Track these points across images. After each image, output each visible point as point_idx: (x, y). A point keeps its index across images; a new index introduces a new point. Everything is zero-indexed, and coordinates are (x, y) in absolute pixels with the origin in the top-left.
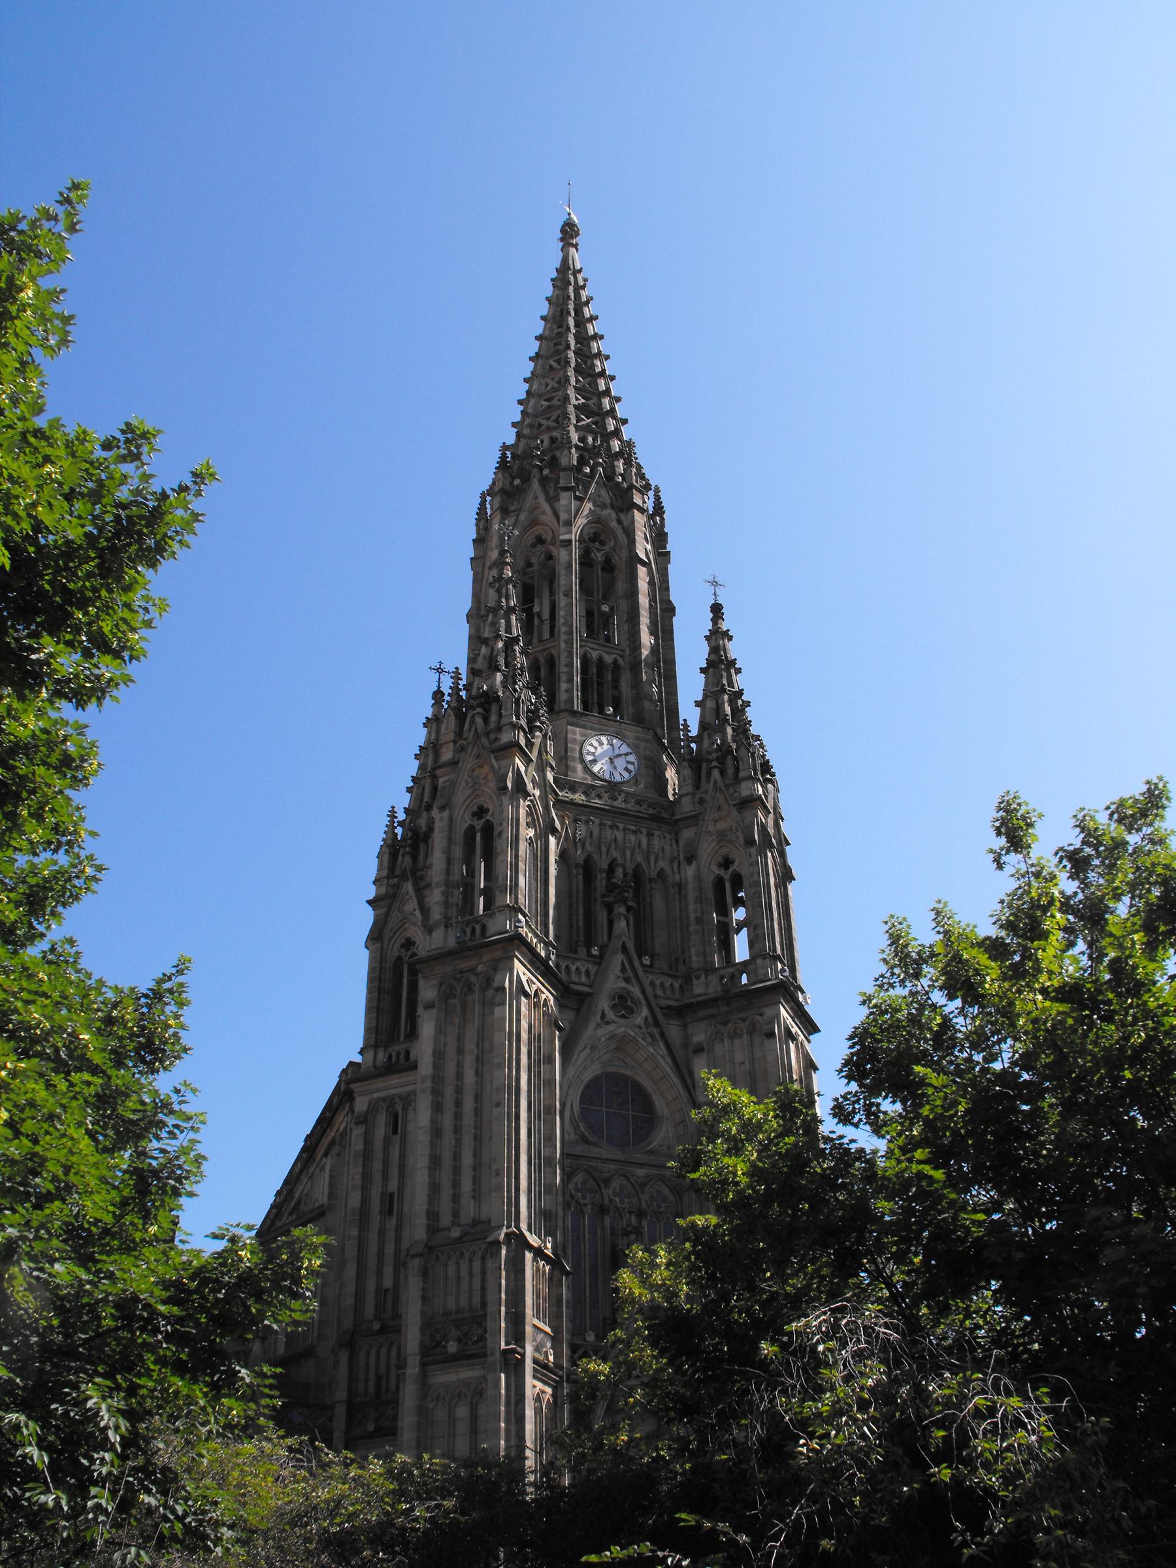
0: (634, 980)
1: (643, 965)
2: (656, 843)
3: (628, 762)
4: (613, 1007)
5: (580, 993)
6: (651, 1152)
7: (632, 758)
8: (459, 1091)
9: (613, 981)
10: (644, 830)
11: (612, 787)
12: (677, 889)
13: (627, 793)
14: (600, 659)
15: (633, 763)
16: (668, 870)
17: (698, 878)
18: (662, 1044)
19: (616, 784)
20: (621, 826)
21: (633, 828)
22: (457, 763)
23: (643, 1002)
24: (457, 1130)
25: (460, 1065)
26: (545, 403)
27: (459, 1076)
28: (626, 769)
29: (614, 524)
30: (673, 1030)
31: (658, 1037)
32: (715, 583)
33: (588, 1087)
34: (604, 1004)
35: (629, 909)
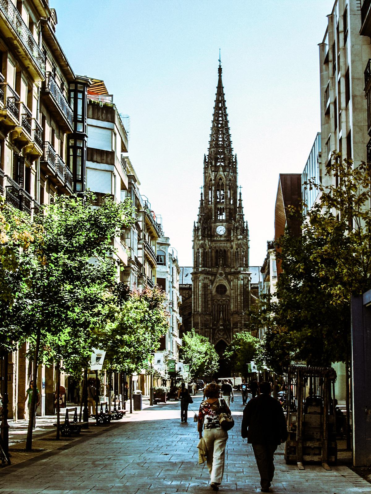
4: (220, 275)
7: (225, 229)
9: (220, 271)
11: (221, 236)
30: (229, 277)
34: (218, 275)
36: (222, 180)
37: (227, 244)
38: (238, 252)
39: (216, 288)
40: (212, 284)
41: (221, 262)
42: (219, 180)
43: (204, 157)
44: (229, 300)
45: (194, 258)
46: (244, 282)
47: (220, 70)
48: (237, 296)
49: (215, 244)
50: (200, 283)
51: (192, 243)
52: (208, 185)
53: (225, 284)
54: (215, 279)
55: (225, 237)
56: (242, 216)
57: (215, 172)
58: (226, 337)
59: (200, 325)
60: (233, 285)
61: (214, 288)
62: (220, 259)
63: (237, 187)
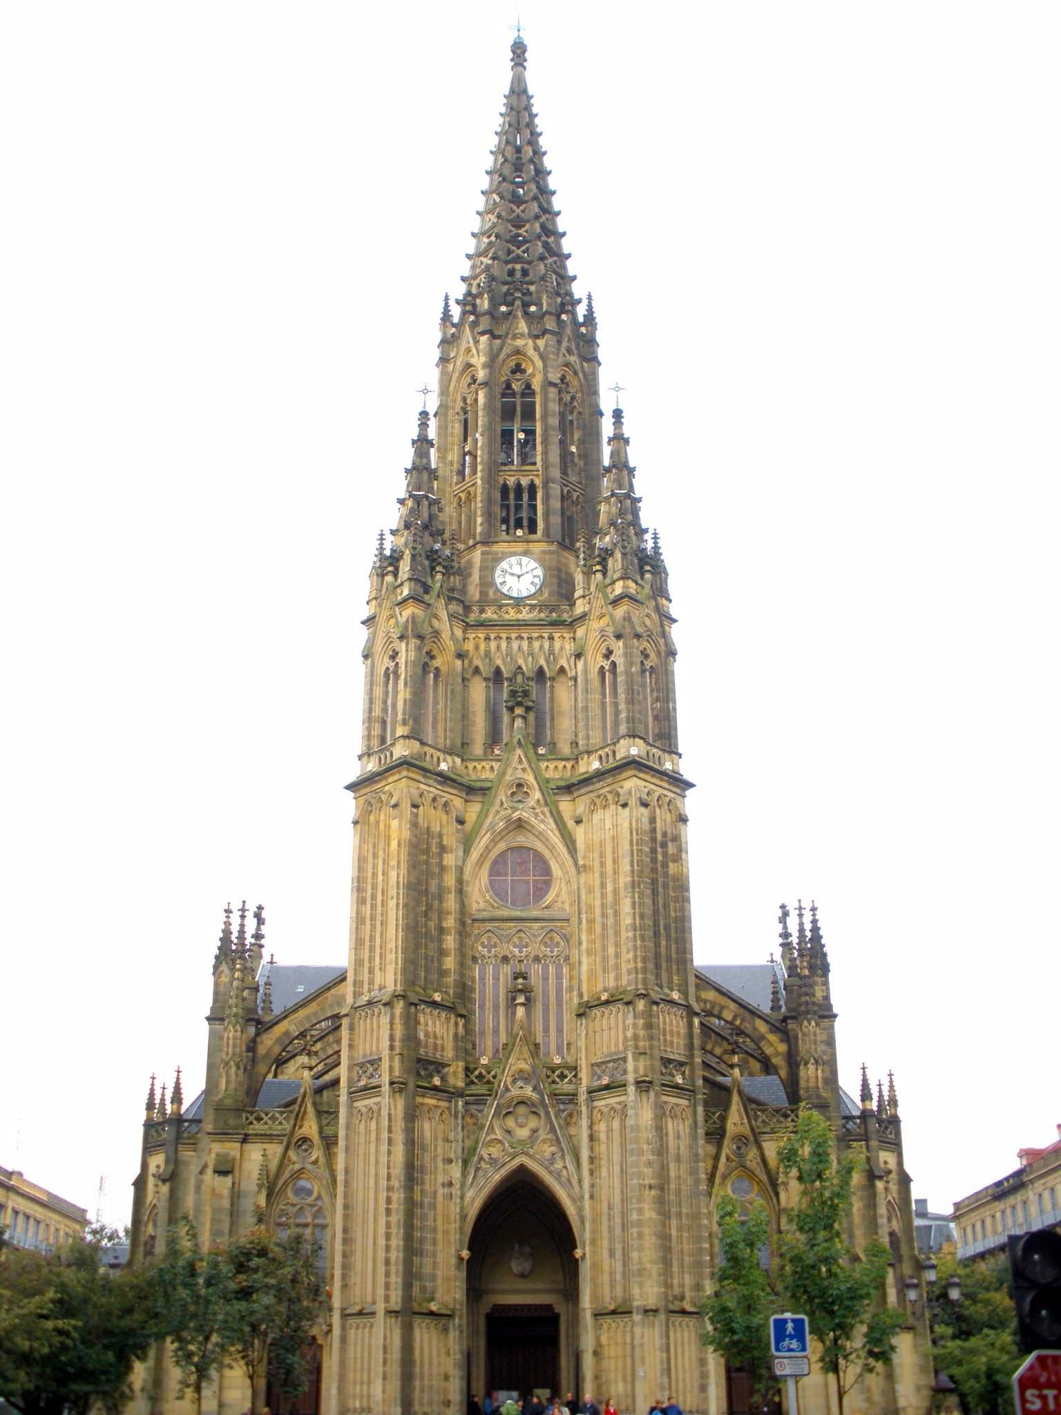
0: (529, 770)
1: (536, 753)
2: (557, 644)
3: (534, 576)
5: (482, 789)
6: (547, 907)
8: (374, 887)
10: (546, 635)
11: (518, 602)
12: (573, 683)
13: (532, 606)
14: (519, 487)
15: (539, 577)
16: (566, 666)
17: (586, 671)
18: (551, 821)
19: (522, 598)
20: (525, 636)
21: (536, 635)
22: (375, 617)
23: (536, 787)
24: (373, 918)
25: (375, 867)
26: (486, 240)
27: (374, 875)
28: (532, 583)
29: (531, 352)
30: (566, 806)
31: (548, 814)
32: (617, 389)
33: (495, 862)
34: (502, 796)
35: (528, 709)
36: (523, 372)
37: (551, 638)
38: (614, 664)
39: (494, 872)
40: (467, 843)
41: (519, 723)
42: (513, 372)
43: (442, 304)
44: (567, 939)
45: (371, 701)
46: (653, 820)
47: (519, 52)
48: (616, 902)
49: (487, 638)
50: (395, 824)
51: (363, 633)
52: (459, 404)
53: (539, 846)
54: (482, 815)
55: (541, 607)
56: (629, 505)
57: (494, 337)
58: (549, 1150)
59: (385, 1064)
60: (589, 848)
61: (479, 863)
62: (511, 709)
63: (601, 414)
